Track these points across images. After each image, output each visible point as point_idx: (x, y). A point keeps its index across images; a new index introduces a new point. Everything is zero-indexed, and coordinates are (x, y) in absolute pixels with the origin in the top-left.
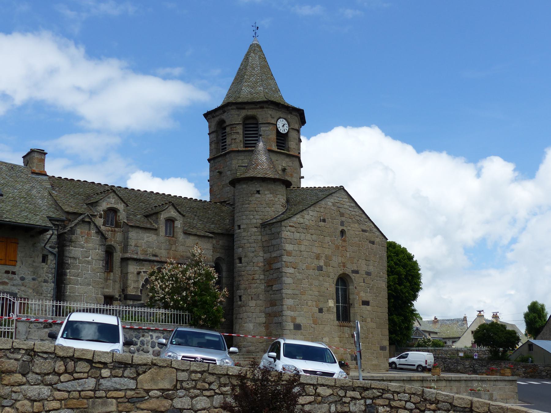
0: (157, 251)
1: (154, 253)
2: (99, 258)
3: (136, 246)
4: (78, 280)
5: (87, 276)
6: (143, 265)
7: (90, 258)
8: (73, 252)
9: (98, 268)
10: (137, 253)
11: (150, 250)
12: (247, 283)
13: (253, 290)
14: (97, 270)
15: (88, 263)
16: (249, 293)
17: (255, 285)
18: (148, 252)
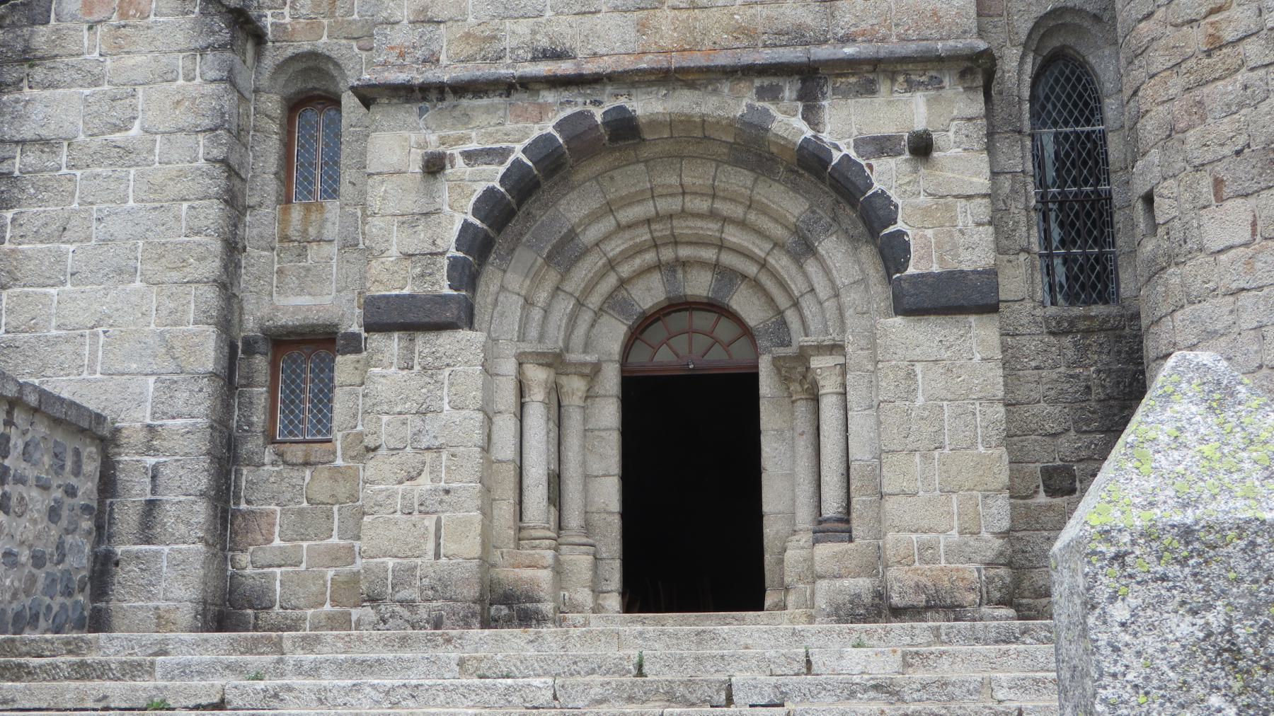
0: (564, 29)
1: (544, 42)
2: (190, 120)
3: (425, 20)
4: (60, 258)
5: (116, 227)
6: (466, 118)
7: (135, 130)
8: (37, 112)
9: (182, 174)
10: (432, 60)
11: (517, 33)
12: (1176, 84)
13: (1226, 127)
14: (173, 190)
15: (126, 153)
16: (1199, 156)
17: (1230, 88)
18: (509, 43)
